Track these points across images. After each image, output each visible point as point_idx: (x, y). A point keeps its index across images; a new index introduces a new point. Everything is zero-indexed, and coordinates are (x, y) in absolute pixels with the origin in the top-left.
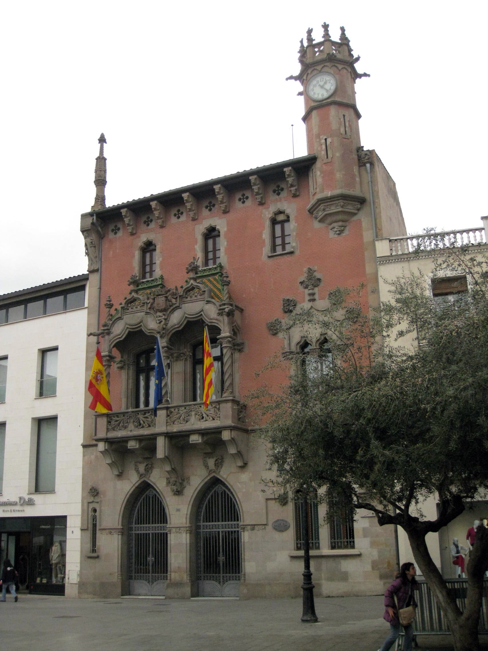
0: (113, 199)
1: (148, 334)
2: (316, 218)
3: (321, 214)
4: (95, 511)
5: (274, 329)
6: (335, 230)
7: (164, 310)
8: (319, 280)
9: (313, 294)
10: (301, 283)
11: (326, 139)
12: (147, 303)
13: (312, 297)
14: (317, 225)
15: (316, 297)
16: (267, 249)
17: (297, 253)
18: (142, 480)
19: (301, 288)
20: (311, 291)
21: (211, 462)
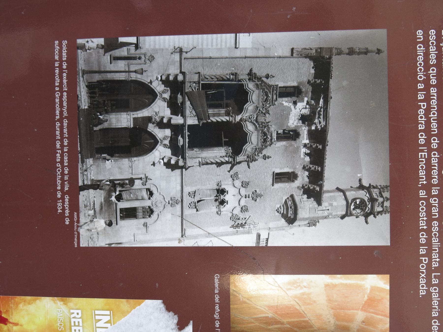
0: (336, 61)
1: (245, 107)
2: (288, 198)
3: (290, 203)
4: (140, 58)
5: (235, 177)
6: (280, 209)
7: (256, 121)
8: (256, 201)
9: (249, 197)
10: (256, 191)
11: (328, 210)
12: (263, 108)
13: (247, 196)
14: (285, 198)
15: (247, 198)
16: (278, 171)
17: (272, 187)
18: (158, 94)
19: (253, 190)
20: (251, 196)
21: (167, 142)
